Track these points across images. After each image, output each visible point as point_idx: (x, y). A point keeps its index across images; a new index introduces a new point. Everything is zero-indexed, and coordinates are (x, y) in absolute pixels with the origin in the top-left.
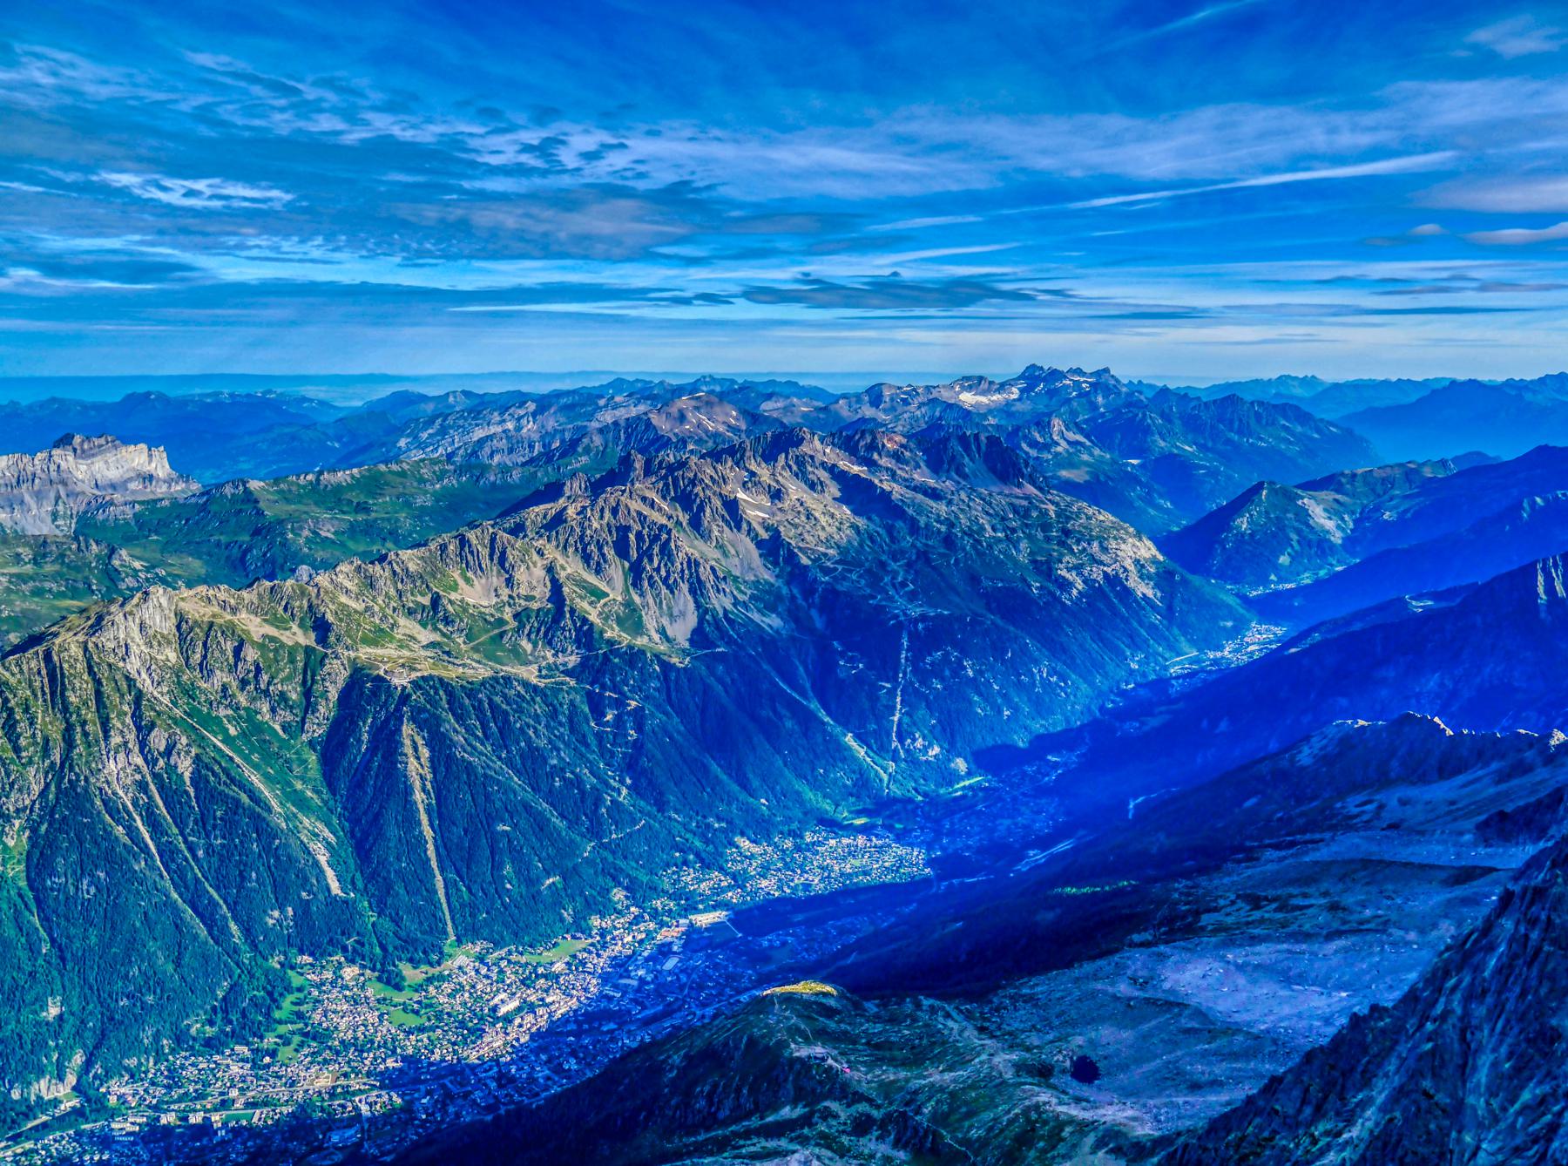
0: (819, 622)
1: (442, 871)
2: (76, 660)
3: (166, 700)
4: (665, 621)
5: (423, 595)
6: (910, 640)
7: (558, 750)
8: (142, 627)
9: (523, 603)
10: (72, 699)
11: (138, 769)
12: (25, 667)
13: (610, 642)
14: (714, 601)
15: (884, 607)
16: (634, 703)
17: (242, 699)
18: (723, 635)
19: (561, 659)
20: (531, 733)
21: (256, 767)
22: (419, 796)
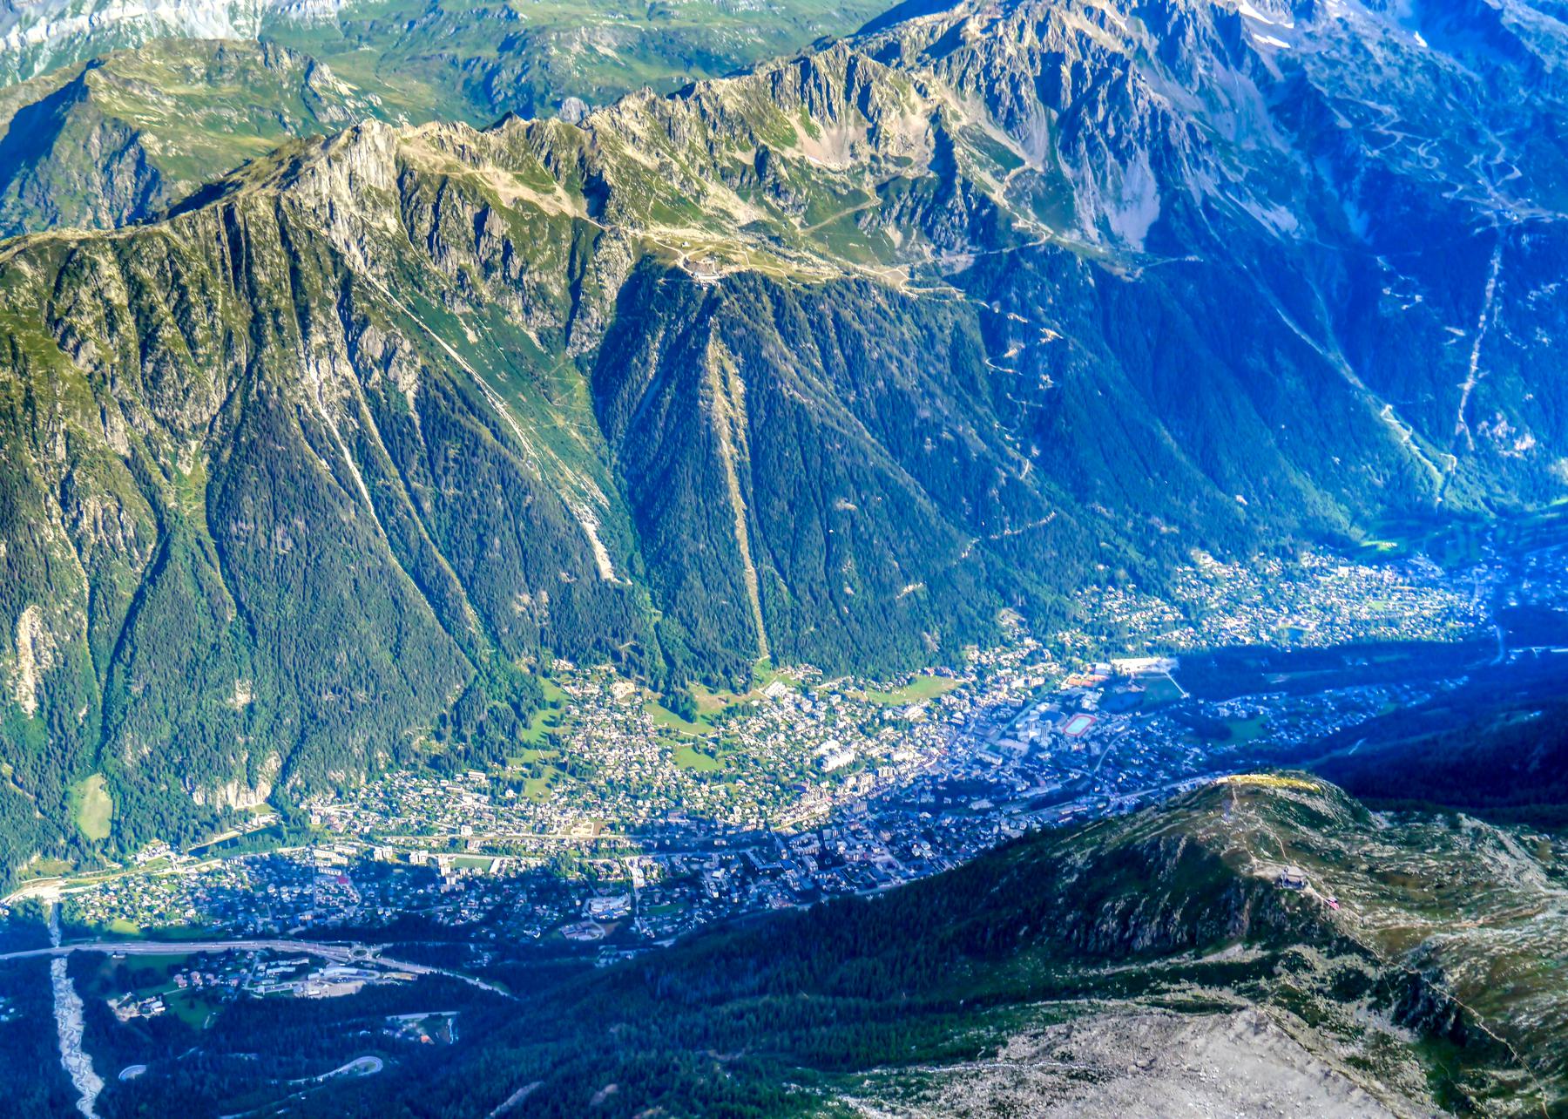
0: (1356, 222)
1: (756, 560)
2: (266, 223)
3: (383, 286)
4: (1108, 209)
5: (743, 149)
6: (1503, 262)
7: (932, 396)
8: (352, 179)
9: (892, 168)
10: (262, 277)
11: (346, 382)
12: (200, 230)
13: (1022, 237)
14: (1189, 181)
15: (1468, 204)
16: (1051, 334)
17: (485, 291)
18: (1200, 236)
19: (945, 258)
20: (894, 367)
21: (502, 390)
22: (726, 449)
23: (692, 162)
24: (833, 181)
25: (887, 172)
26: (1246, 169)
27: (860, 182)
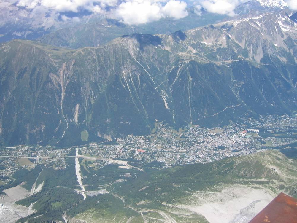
5: (195, 41)
9: (219, 46)
10: (117, 56)
11: (129, 73)
23: (186, 43)
24: (209, 47)
25: (218, 46)
26: (278, 50)
27: (213, 48)
